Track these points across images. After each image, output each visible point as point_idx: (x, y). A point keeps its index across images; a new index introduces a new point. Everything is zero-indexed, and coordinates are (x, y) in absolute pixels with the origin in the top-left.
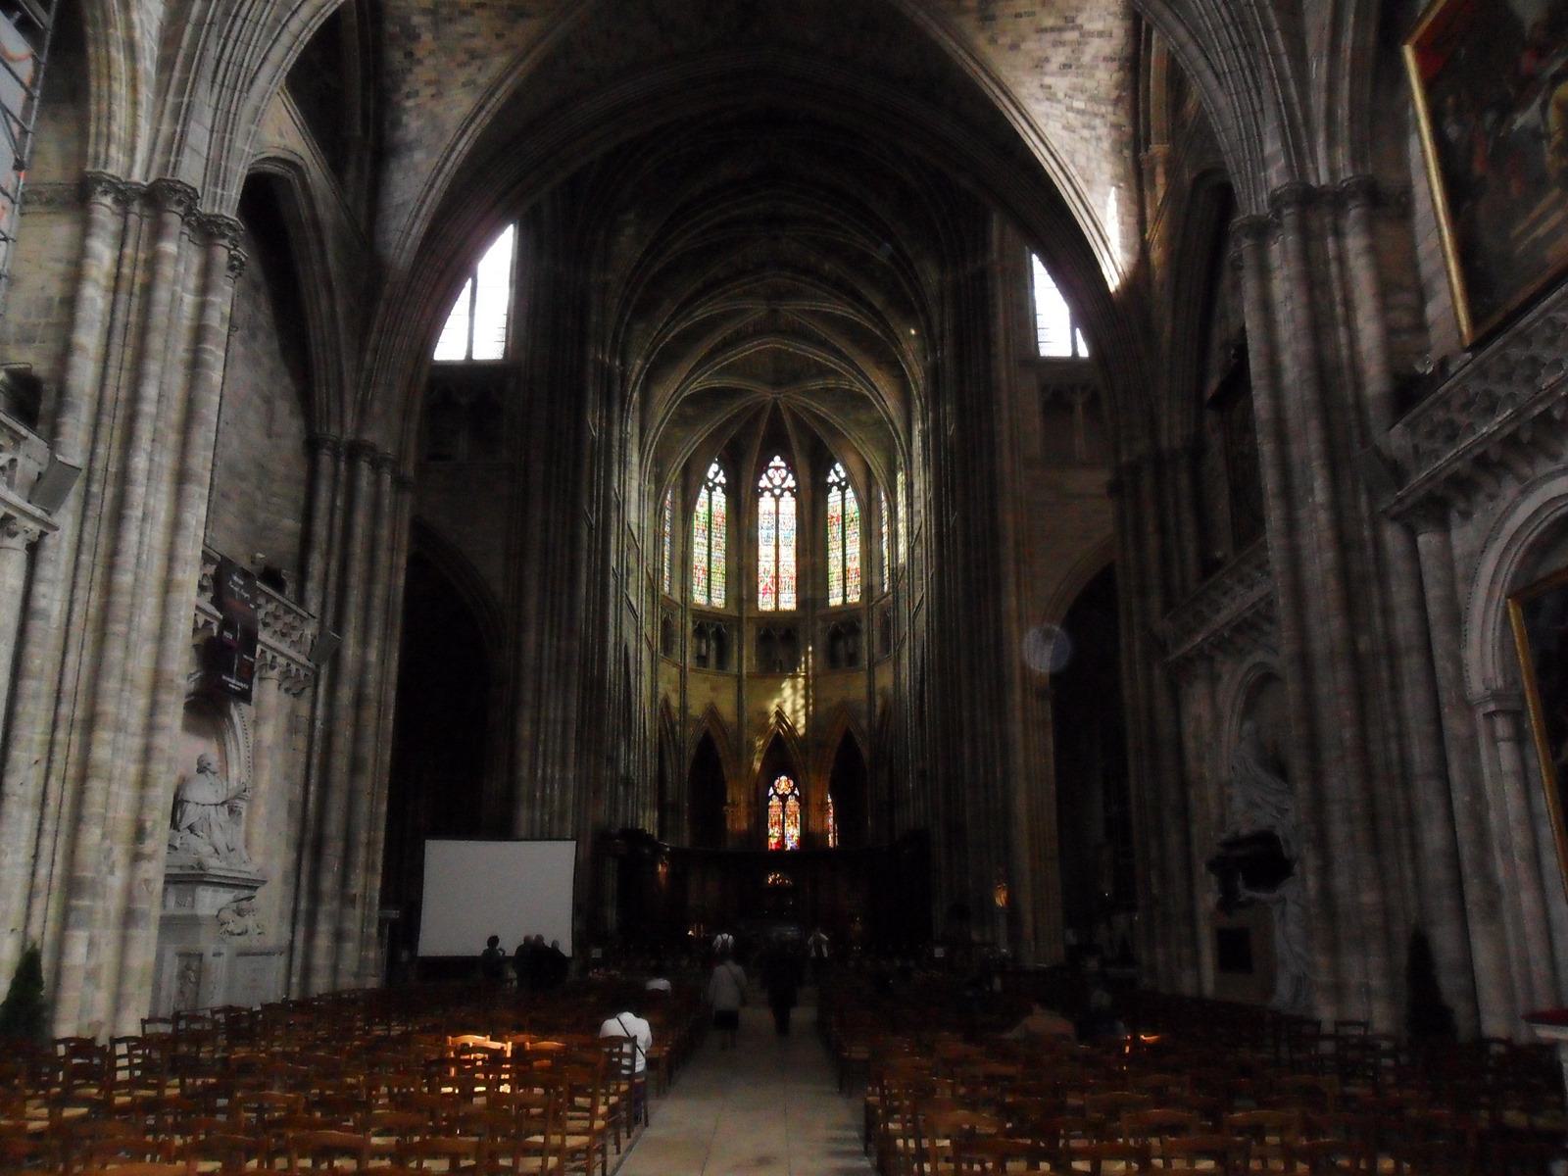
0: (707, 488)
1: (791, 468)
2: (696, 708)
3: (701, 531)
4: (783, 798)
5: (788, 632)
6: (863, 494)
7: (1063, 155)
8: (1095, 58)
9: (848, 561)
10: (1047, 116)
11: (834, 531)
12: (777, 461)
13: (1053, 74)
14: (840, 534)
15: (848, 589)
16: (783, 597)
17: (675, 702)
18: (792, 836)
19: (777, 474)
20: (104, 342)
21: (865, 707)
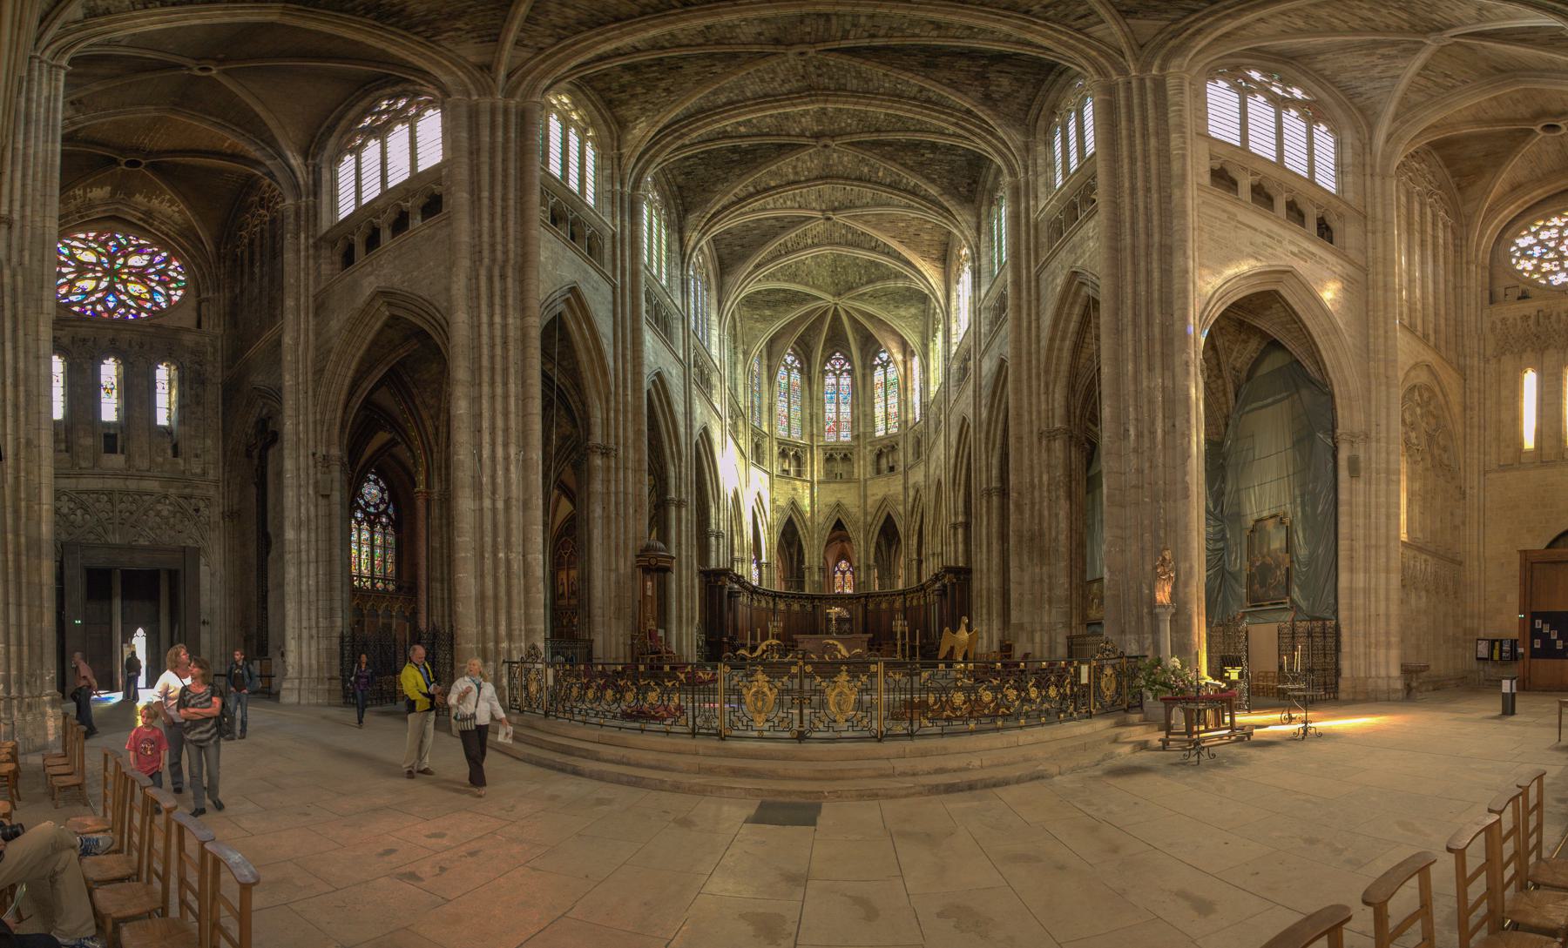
1: (848, 359)
5: (845, 455)
11: (879, 392)
16: (842, 434)
19: (838, 362)
21: (901, 498)
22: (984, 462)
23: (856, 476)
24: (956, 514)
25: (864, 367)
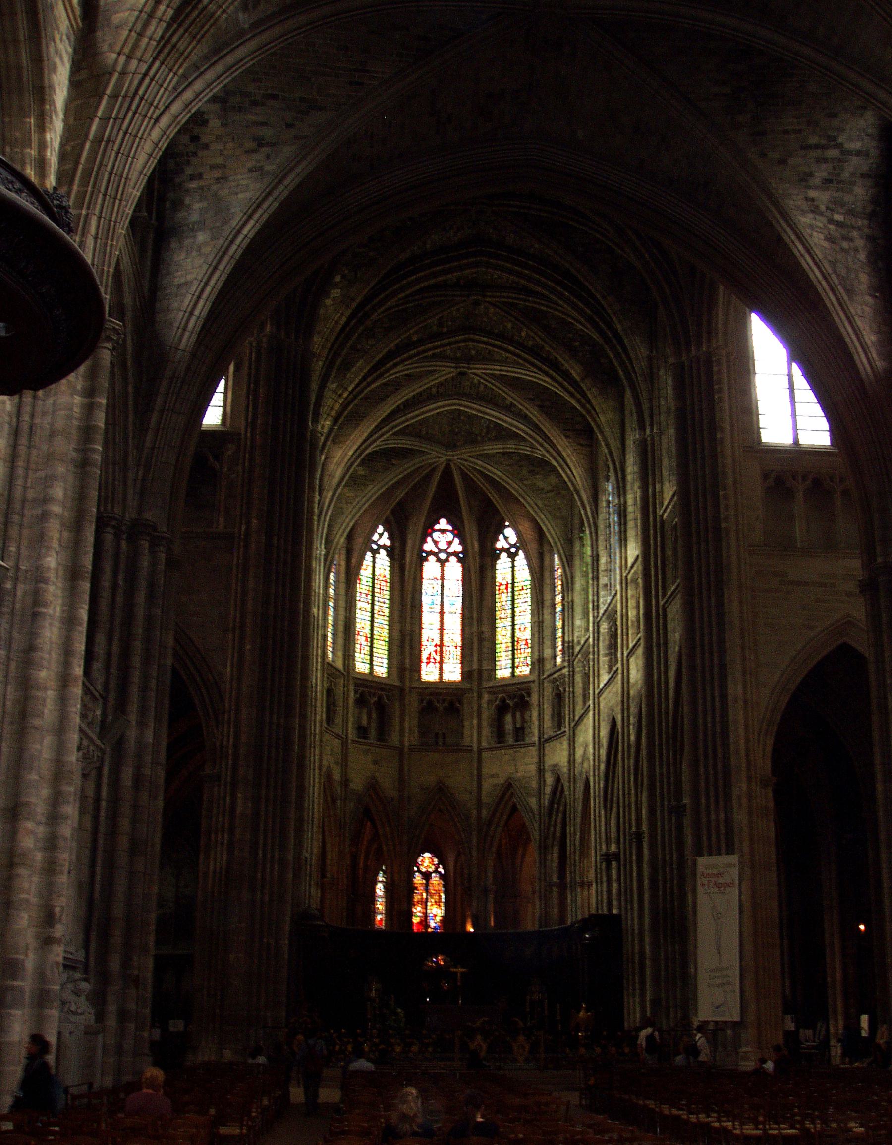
1: (458, 532)
2: (357, 783)
3: (364, 596)
4: (427, 876)
5: (452, 704)
6: (535, 562)
7: (827, 265)
8: (853, 175)
9: (517, 631)
10: (812, 227)
11: (503, 599)
12: (443, 524)
13: (816, 188)
14: (510, 603)
15: (516, 660)
17: (337, 775)
18: (435, 916)
20: (12, 441)
21: (534, 784)
22: (633, 799)
23: (466, 741)
24: (608, 842)
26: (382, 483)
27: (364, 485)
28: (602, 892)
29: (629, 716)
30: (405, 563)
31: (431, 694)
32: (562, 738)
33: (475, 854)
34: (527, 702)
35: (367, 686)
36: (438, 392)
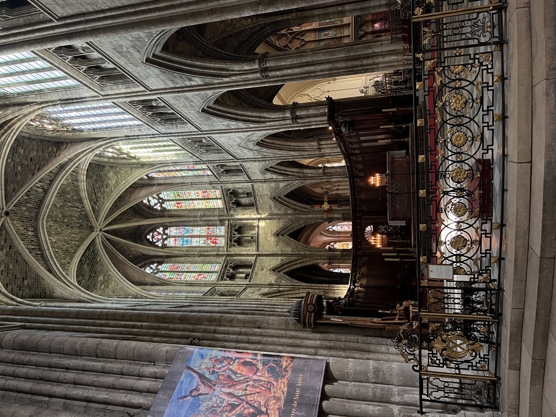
0: (157, 273)
1: (153, 228)
2: (272, 278)
3: (178, 277)
5: (236, 230)
11: (185, 205)
15: (213, 197)
17: (265, 290)
21: (273, 184)
24: (284, 119)
25: (163, 216)
26: (109, 266)
27: (108, 277)
28: (316, 121)
29: (187, 87)
30: (166, 255)
31: (231, 241)
32: (246, 168)
33: (310, 216)
34: (233, 190)
35: (224, 274)
36: (32, 231)
